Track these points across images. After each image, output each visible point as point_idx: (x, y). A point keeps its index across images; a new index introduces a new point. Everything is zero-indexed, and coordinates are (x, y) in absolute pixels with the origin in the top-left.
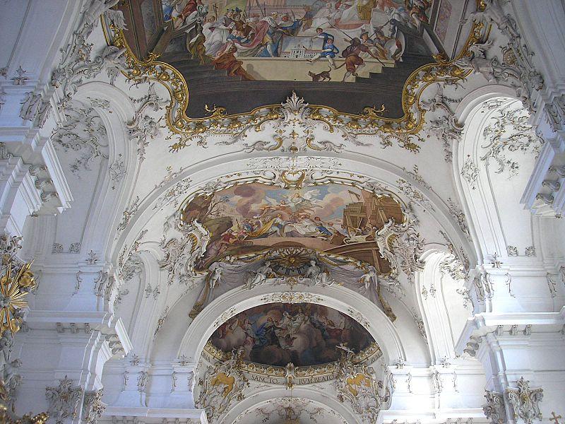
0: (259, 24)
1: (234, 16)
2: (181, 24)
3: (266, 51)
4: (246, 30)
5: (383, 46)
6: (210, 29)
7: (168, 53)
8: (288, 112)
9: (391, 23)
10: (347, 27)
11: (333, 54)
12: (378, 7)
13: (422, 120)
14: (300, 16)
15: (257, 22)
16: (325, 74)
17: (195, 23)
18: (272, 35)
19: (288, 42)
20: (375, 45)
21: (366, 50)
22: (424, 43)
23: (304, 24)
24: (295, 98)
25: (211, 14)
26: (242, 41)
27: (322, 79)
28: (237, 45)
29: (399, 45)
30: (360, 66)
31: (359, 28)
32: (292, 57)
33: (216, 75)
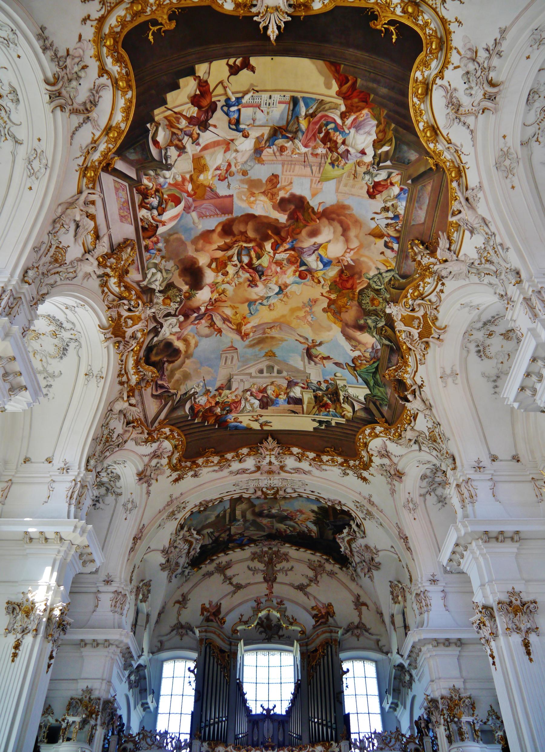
0: (312, 144)
1: (337, 159)
2: (393, 175)
3: (307, 106)
4: (327, 139)
5: (173, 134)
6: (365, 154)
7: (416, 151)
8: (282, 7)
9: (170, 164)
10: (216, 144)
11: (228, 103)
12: (188, 176)
13: (99, 57)
14: (268, 153)
15: (315, 148)
16: (234, 70)
17: (380, 169)
18: (298, 130)
19: (281, 118)
20: (181, 130)
21: (191, 120)
22: (130, 163)
23: (263, 142)
24: (273, 33)
25: (361, 170)
26: (332, 126)
27: (239, 61)
28: (339, 121)
29: (156, 143)
30: (193, 94)
31: (202, 145)
32: (277, 96)
33: (371, 85)
